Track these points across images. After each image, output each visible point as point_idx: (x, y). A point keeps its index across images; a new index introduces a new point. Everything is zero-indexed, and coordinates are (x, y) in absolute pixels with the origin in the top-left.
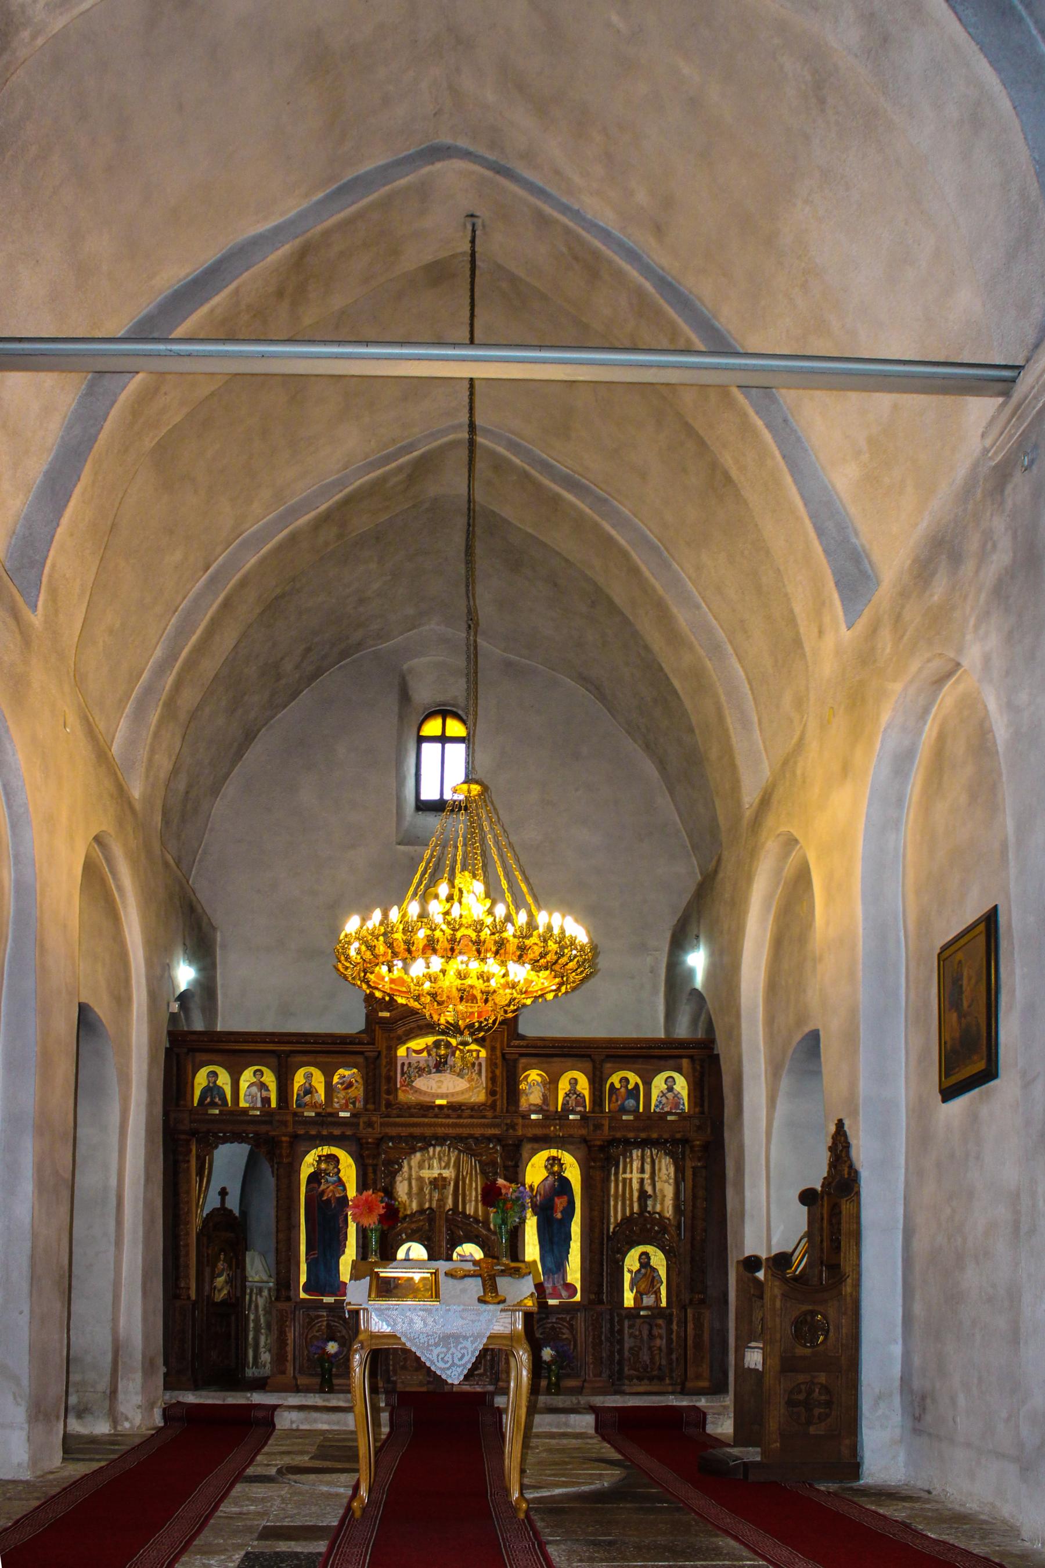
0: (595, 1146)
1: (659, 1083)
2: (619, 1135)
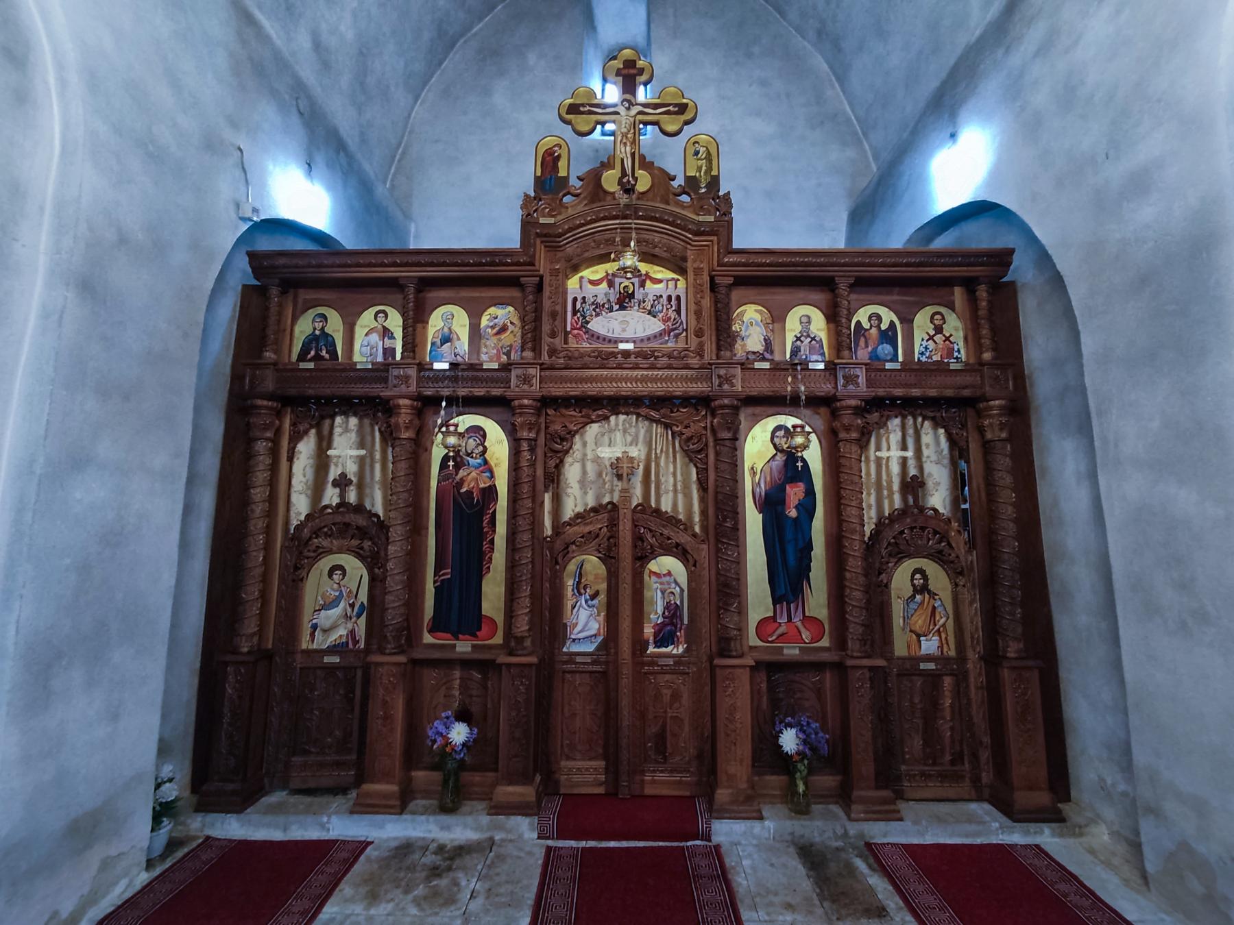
0: (849, 407)
2: (881, 392)
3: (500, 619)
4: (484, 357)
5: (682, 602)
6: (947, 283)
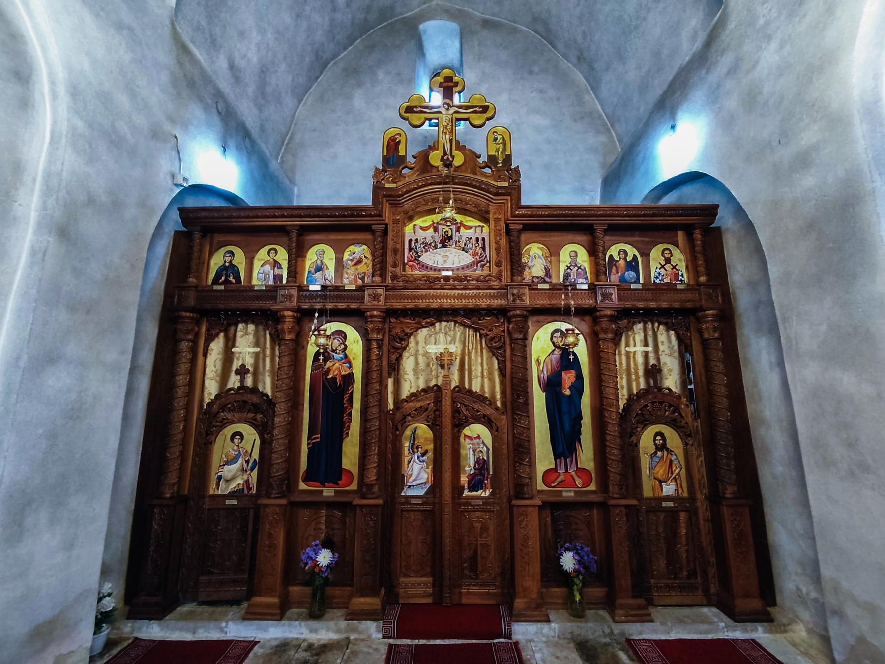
2: (628, 305)
3: (355, 471)
4: (345, 281)
5: (488, 458)
6: (674, 228)
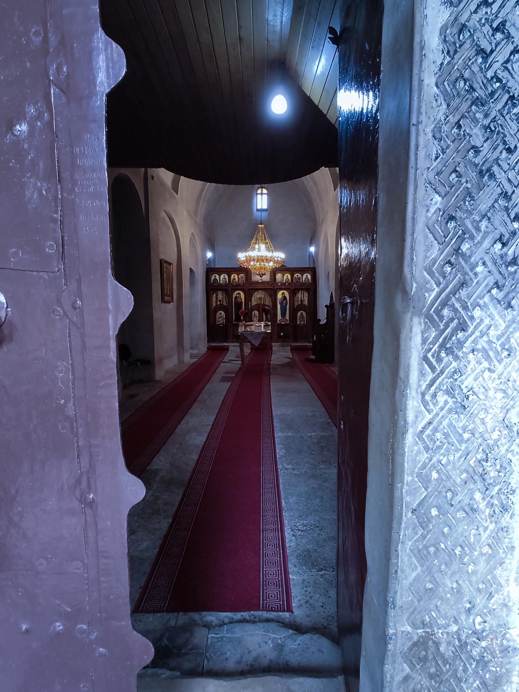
1: (305, 276)
